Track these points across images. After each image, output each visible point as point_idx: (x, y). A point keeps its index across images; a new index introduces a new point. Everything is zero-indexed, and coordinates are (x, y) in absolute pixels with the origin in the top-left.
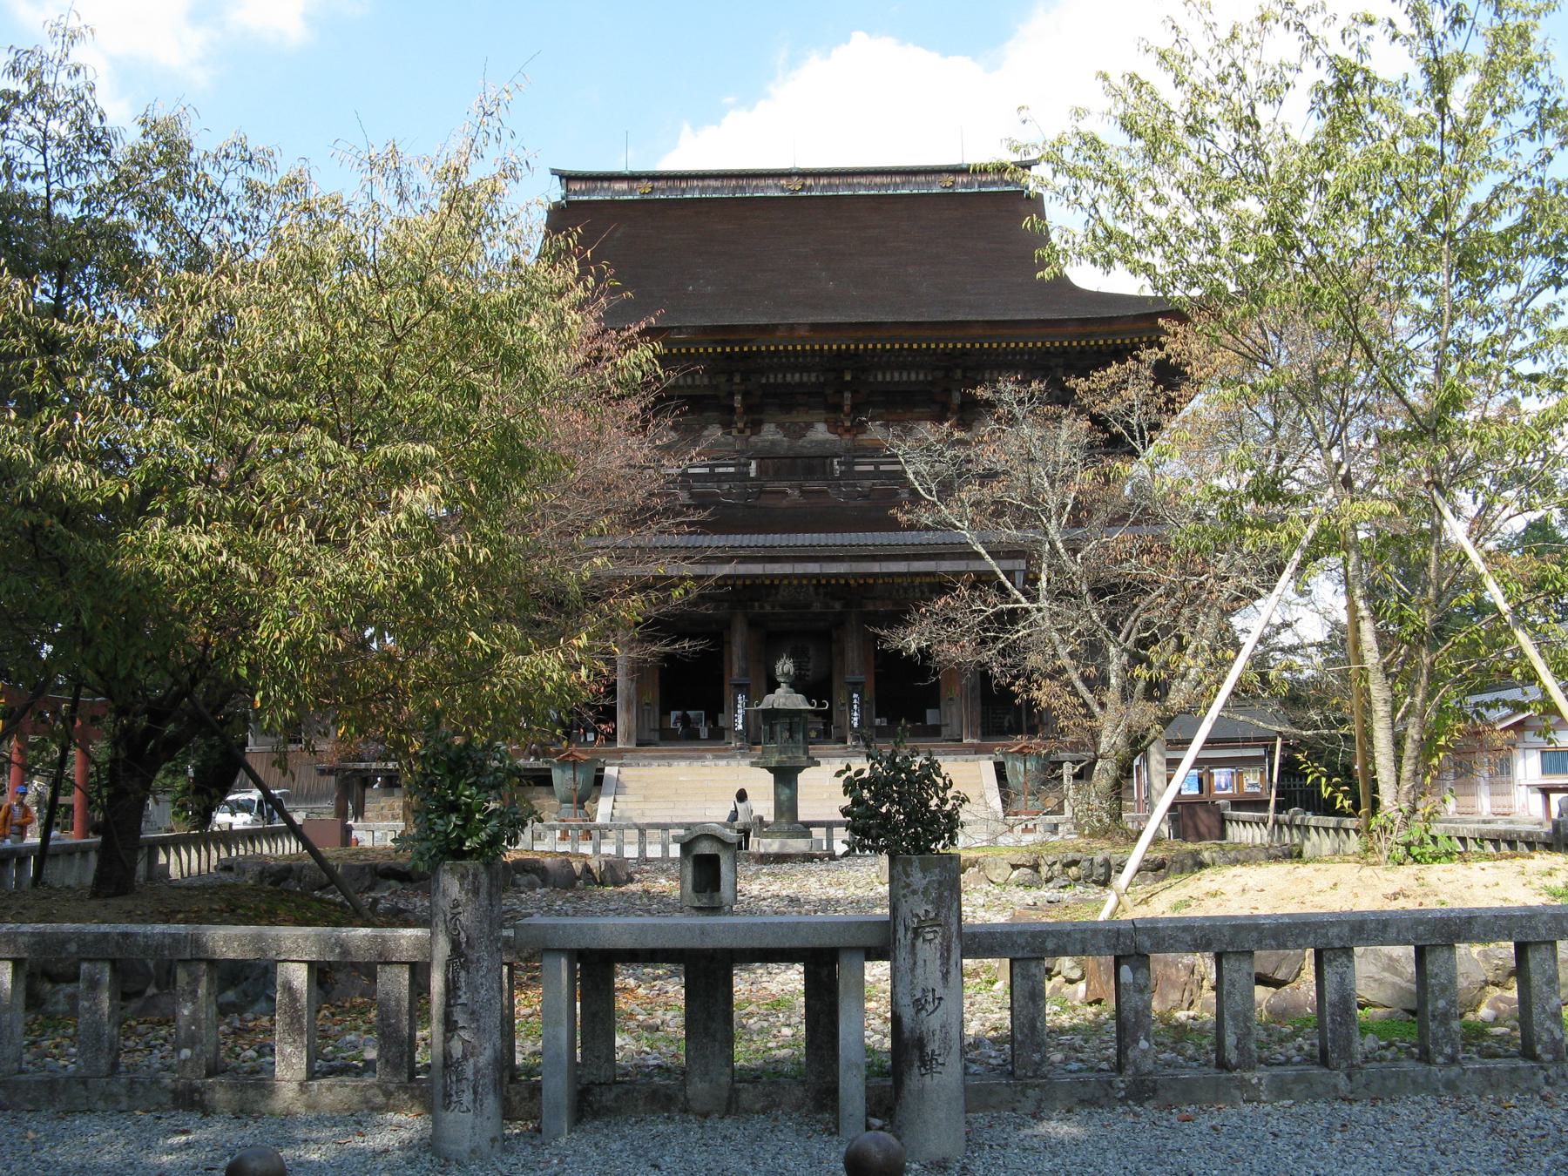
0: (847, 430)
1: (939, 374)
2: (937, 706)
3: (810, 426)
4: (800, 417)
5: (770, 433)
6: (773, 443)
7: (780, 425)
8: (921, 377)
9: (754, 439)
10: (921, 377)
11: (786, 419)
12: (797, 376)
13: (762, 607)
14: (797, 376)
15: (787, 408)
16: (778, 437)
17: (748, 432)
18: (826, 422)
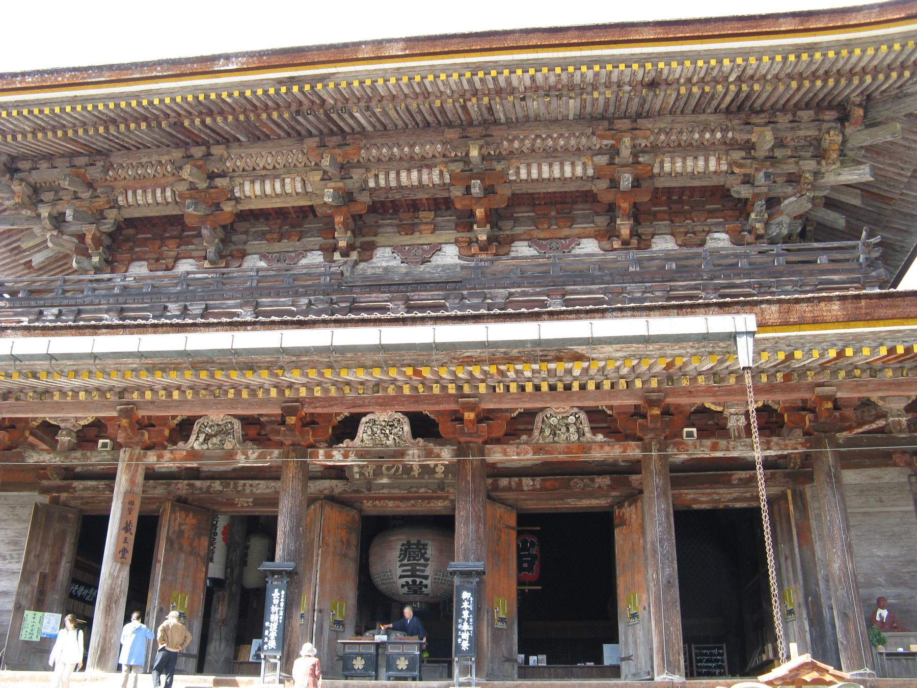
0: (484, 249)
1: (603, 160)
2: (613, 638)
3: (436, 248)
4: (425, 238)
5: (385, 259)
6: (386, 269)
7: (396, 249)
8: (579, 171)
9: (362, 265)
10: (579, 171)
11: (406, 240)
12: (414, 174)
13: (329, 456)
14: (414, 174)
15: (410, 229)
16: (393, 263)
17: (354, 255)
18: (456, 242)
